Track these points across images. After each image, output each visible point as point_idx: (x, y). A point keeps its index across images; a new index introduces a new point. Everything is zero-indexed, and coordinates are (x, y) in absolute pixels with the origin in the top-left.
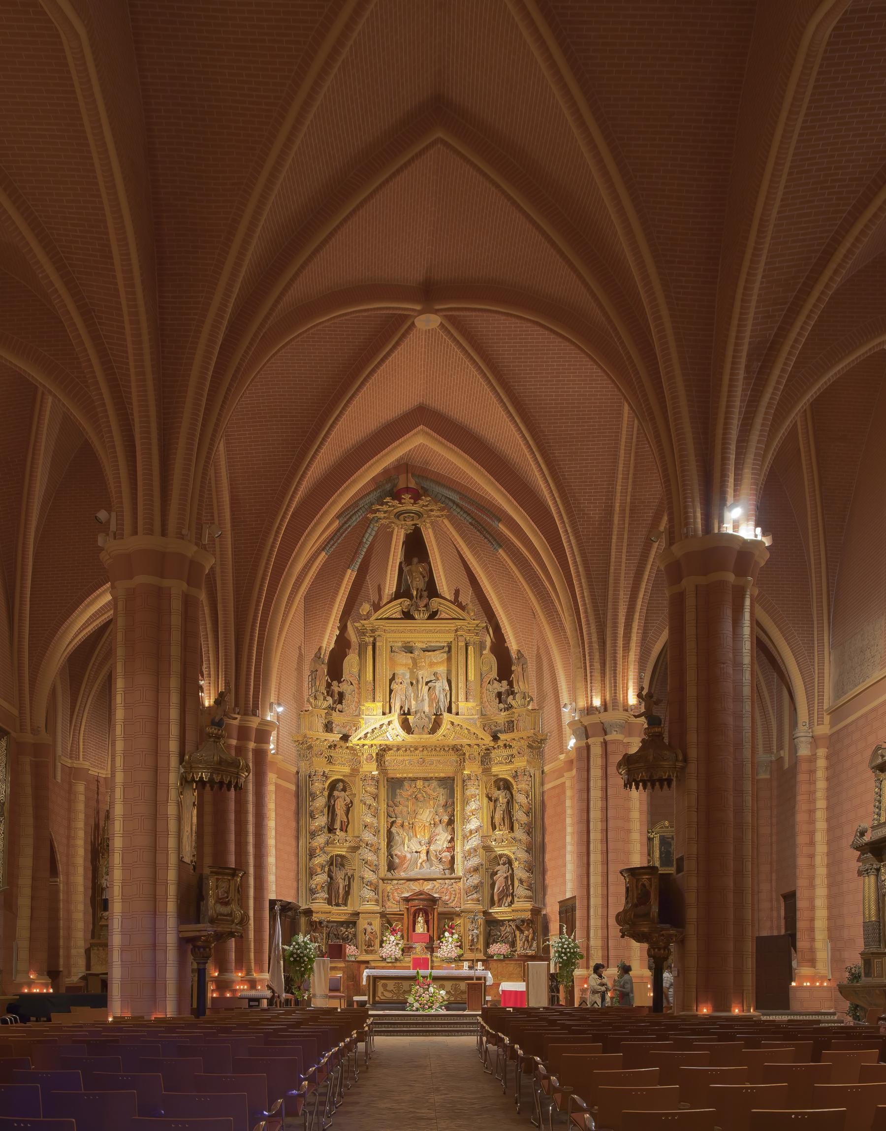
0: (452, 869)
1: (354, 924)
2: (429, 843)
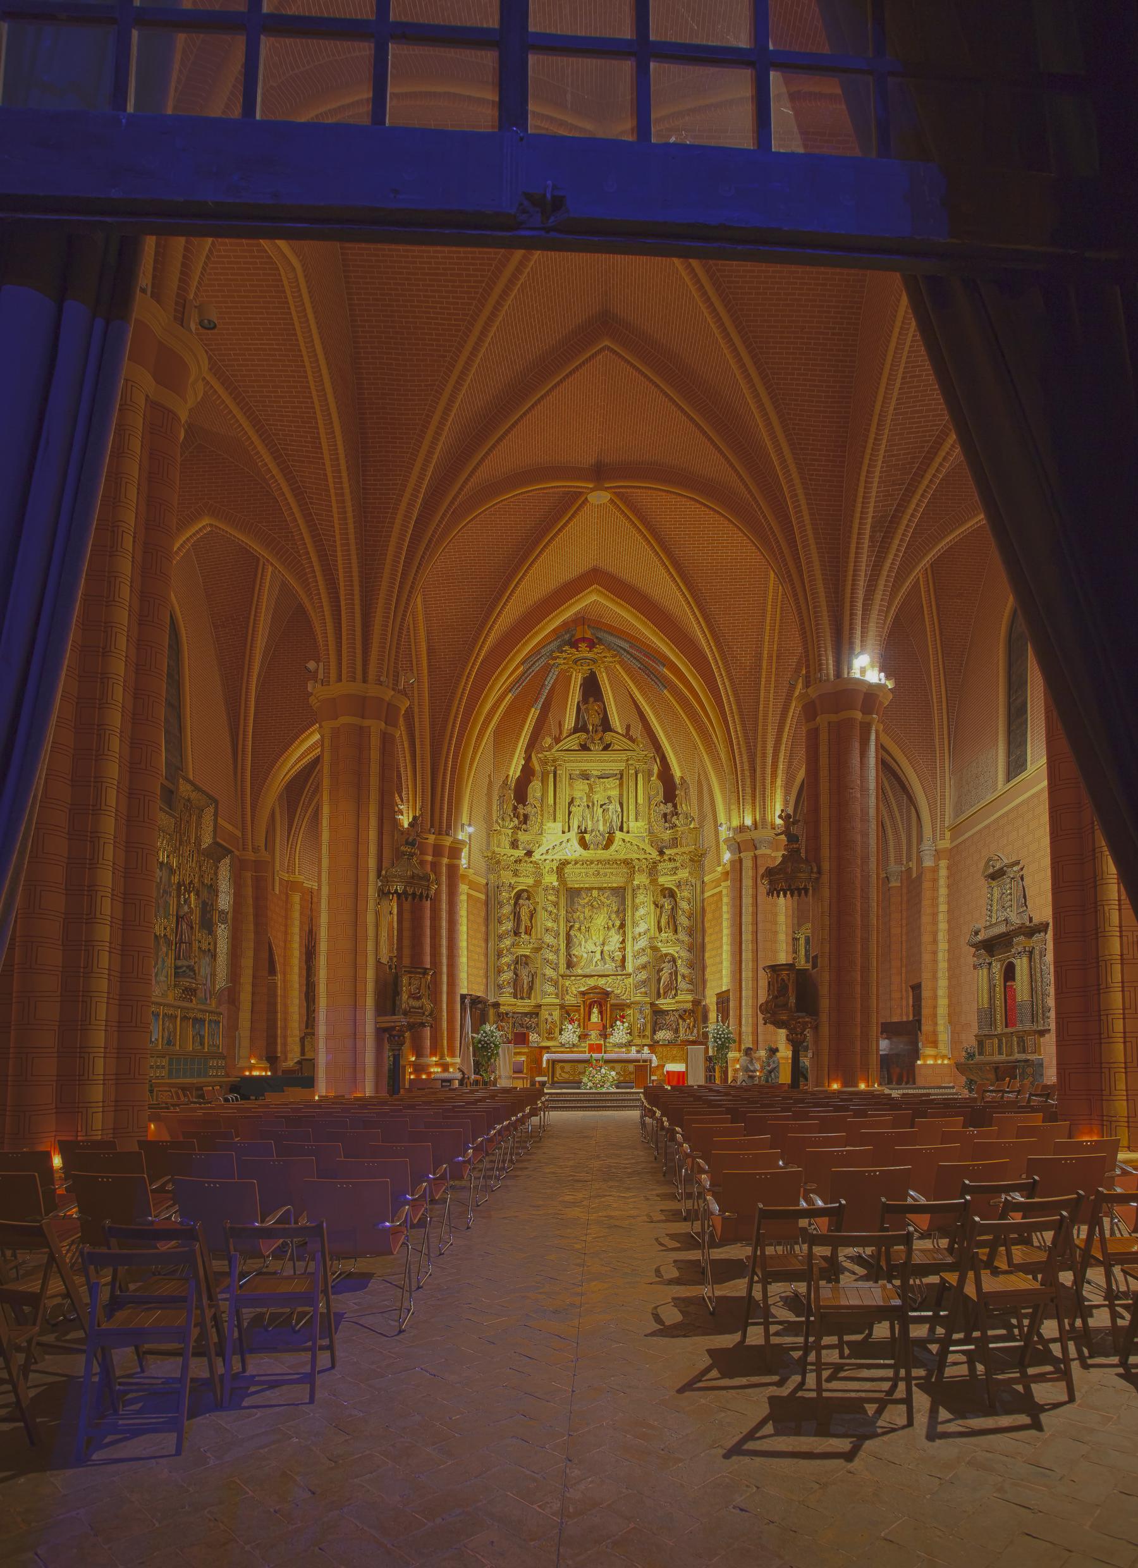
0: (623, 967)
1: (537, 1014)
2: (603, 944)
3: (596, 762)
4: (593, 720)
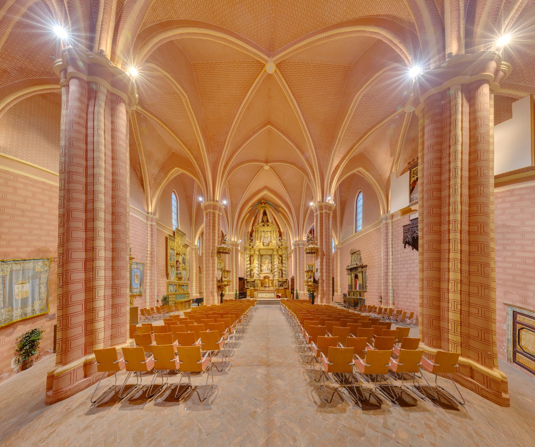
3: (266, 229)
4: (265, 220)
